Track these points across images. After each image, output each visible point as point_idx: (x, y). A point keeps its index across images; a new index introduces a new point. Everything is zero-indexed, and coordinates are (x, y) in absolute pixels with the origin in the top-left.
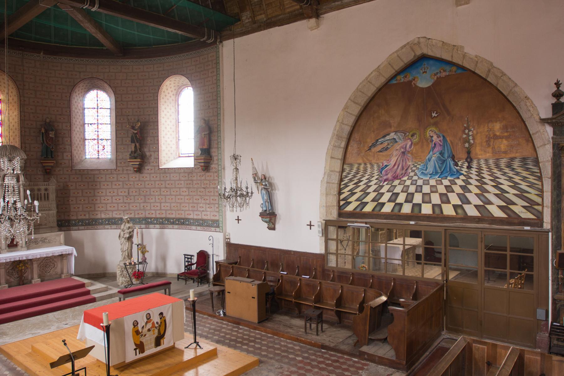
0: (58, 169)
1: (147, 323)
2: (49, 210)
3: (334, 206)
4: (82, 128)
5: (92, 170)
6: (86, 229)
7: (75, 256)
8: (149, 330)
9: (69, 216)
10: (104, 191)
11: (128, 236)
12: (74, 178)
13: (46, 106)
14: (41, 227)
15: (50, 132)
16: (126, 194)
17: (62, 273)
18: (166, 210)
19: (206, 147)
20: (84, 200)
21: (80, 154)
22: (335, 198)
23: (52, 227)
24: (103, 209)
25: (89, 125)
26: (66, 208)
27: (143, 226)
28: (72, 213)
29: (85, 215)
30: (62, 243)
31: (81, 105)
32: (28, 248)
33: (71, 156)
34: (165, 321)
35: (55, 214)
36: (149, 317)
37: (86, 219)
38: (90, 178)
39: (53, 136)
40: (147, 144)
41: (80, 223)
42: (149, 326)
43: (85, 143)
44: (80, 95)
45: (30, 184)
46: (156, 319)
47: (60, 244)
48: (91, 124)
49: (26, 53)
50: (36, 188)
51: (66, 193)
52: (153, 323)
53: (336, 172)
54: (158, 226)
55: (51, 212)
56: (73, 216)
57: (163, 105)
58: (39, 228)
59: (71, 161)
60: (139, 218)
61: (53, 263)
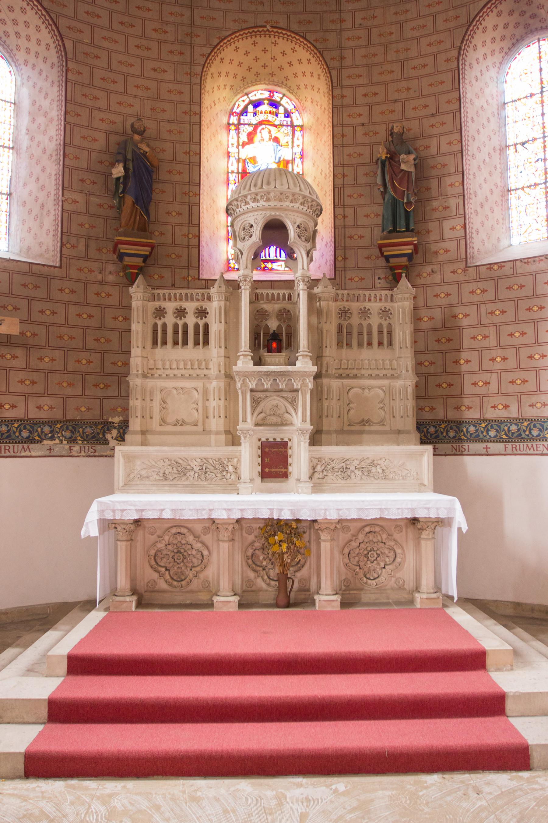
0: (428, 269)
5: (526, 261)
6: (509, 451)
7: (460, 529)
9: (458, 408)
12: (473, 292)
13: (396, 101)
14: (367, 428)
15: (403, 156)
17: (417, 589)
20: (504, 359)
21: (493, 228)
23: (399, 432)
25: (519, 147)
26: (450, 385)
28: (467, 401)
29: (506, 407)
30: (426, 483)
32: (317, 488)
35: (410, 390)
37: (511, 421)
38: (521, 287)
39: (412, 169)
41: (492, 433)
47: (420, 488)
48: (523, 144)
50: (355, 306)
51: (449, 340)
55: (399, 383)
56: (469, 408)
58: (361, 432)
59: (463, 242)
61: (392, 549)
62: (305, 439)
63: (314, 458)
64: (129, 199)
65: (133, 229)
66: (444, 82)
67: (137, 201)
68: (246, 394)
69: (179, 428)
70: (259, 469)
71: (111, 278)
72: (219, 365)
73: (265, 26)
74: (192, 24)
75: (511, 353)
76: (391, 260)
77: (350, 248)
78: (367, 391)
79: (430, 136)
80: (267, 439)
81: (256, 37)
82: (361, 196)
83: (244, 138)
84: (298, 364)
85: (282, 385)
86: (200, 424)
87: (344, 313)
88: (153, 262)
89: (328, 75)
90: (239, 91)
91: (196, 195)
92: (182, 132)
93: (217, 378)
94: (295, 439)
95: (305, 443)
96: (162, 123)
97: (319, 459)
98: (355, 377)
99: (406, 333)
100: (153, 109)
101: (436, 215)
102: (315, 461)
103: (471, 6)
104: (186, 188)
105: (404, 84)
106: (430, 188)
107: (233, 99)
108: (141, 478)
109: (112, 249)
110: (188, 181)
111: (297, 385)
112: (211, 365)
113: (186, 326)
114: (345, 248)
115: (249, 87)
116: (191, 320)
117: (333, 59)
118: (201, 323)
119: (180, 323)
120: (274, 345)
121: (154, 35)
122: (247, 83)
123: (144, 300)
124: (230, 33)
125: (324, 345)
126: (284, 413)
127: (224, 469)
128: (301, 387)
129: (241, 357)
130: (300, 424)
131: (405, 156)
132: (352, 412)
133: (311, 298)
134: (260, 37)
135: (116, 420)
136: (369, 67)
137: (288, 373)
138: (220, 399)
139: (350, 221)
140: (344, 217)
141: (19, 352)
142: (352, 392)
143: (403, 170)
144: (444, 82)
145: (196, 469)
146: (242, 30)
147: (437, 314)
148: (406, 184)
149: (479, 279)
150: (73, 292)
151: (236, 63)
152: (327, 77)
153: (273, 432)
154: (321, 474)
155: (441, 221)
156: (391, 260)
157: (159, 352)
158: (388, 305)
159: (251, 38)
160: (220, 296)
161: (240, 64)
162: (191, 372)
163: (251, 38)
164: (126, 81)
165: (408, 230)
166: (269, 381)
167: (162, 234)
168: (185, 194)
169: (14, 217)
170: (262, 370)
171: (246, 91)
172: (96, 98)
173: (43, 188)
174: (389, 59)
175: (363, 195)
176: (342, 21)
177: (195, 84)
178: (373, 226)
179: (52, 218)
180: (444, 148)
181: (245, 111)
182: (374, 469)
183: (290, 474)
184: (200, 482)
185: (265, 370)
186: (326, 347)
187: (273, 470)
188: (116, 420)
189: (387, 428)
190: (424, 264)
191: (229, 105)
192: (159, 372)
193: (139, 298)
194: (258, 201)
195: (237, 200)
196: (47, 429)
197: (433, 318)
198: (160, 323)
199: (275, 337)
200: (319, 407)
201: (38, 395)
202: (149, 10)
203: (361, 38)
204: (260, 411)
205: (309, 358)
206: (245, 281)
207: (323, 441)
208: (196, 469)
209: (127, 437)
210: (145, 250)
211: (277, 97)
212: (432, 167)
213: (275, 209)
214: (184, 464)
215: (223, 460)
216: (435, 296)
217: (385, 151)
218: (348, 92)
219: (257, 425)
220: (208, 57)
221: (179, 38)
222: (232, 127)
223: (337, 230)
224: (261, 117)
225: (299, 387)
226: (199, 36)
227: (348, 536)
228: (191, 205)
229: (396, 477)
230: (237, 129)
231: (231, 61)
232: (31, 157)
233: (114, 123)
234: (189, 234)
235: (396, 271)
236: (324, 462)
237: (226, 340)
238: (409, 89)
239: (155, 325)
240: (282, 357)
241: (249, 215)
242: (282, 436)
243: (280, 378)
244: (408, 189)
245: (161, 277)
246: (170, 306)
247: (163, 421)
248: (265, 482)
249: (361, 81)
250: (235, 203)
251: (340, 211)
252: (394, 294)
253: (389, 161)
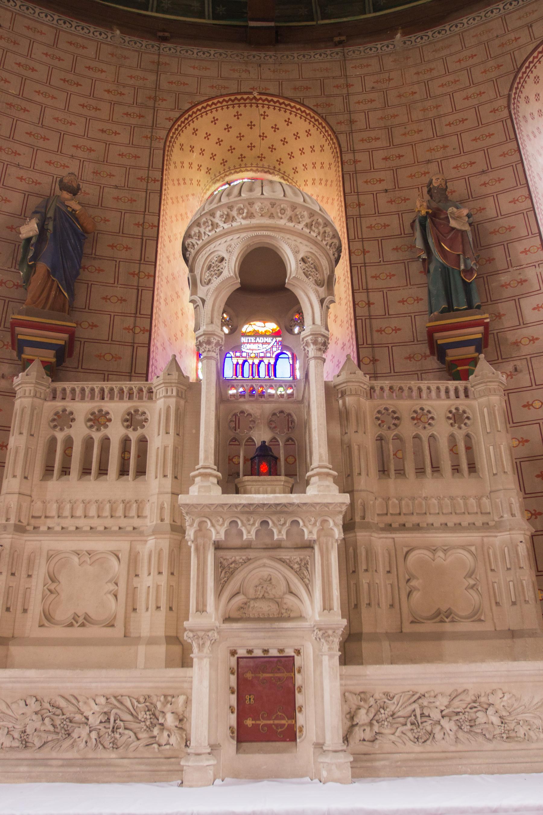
2: (486, 526)
13: (429, 162)
14: (448, 627)
23: (513, 634)
35: (523, 550)
39: (467, 228)
45: (372, 388)
49: (351, 48)
58: (439, 637)
62: (330, 649)
63: (350, 692)
64: (42, 267)
65: (44, 308)
66: (493, 134)
67: (53, 271)
68: (204, 553)
69: (76, 632)
70: (233, 719)
72: (162, 508)
73: (251, 93)
74: (157, 87)
76: (450, 352)
77: (381, 345)
78: (440, 554)
79: (486, 196)
80: (250, 652)
81: (239, 107)
82: (391, 276)
85: (280, 532)
86: (120, 623)
88: (75, 365)
89: (335, 141)
90: (218, 178)
91: (149, 276)
92: (135, 201)
93: (156, 532)
94: (309, 650)
95: (331, 657)
96: (106, 190)
97: (363, 696)
98: (417, 527)
99: (500, 448)
100: (95, 173)
101: (508, 292)
102: (354, 701)
103: (516, 53)
104: (135, 268)
105: (438, 143)
106: (493, 259)
107: (210, 187)
109: (10, 343)
110: (139, 259)
111: (311, 532)
112: (147, 512)
113: (106, 442)
114: (373, 346)
115: (231, 173)
117: (340, 123)
118: (134, 436)
119: (97, 436)
121: (106, 96)
122: (229, 168)
123: (35, 396)
124: (207, 98)
125: (356, 471)
126: (285, 594)
128: (319, 537)
129: (198, 479)
130: (320, 615)
131: (455, 210)
132: (416, 595)
134: (245, 106)
136: (389, 130)
137: (291, 509)
138: (160, 573)
139: (378, 309)
140: (369, 304)
142: (412, 557)
143: (453, 229)
144: (493, 134)
145: (94, 721)
146: (222, 96)
148: (461, 246)
151: (213, 139)
152: (334, 143)
153: (262, 634)
154: (368, 729)
155: (517, 300)
156: (450, 352)
158: (462, 403)
159: (233, 107)
160: (169, 389)
161: (219, 142)
162: (109, 522)
163: (233, 107)
164: (61, 140)
165: (470, 306)
166: (254, 524)
167: (93, 326)
168: (133, 274)
170: (238, 502)
171: (227, 179)
172: (16, 153)
174: (414, 118)
175: (394, 275)
176: (348, 86)
177: (157, 149)
178: (413, 315)
180: (506, 207)
182: (481, 717)
183: (301, 731)
184: (102, 754)
185: (244, 502)
186: (360, 474)
187: (262, 722)
189: (487, 627)
190: (500, 360)
191: (205, 193)
192: (50, 523)
193: (27, 394)
194: (234, 219)
195: (199, 225)
197: (527, 441)
198: (60, 436)
200: (353, 587)
202: (102, 71)
203: (374, 100)
204: (236, 589)
205: (331, 479)
206: (209, 343)
207: (364, 655)
208: (94, 721)
212: (491, 233)
214: (69, 709)
215: (154, 700)
216: (524, 406)
217: (425, 204)
219: (228, 619)
221: (139, 101)
223: (359, 322)
225: (315, 537)
226: (165, 100)
228: (140, 289)
229: (531, 733)
231: (208, 136)
234: (135, 327)
235: (459, 368)
236: (372, 701)
237: (175, 465)
238: (445, 147)
239: (53, 441)
241: (219, 242)
242: (281, 643)
243: (274, 518)
244: (464, 253)
248: (245, 752)
249: (378, 144)
250: (196, 230)
251: (361, 297)
252: (469, 386)
253: (432, 220)
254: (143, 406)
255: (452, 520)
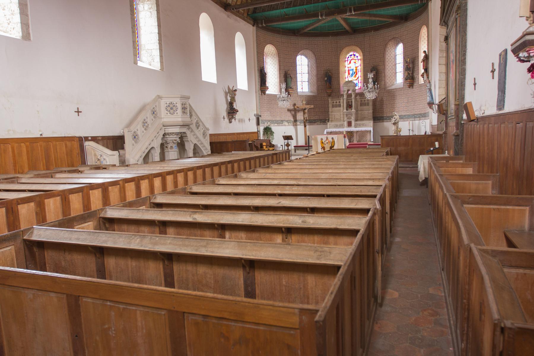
1: (326, 140)
3: (443, 95)
4: (394, 66)
5: (393, 89)
8: (327, 143)
9: (383, 114)
10: (398, 100)
11: (393, 122)
16: (407, 101)
18: (421, 109)
19: (424, 68)
22: (444, 89)
23: (370, 119)
24: (397, 110)
26: (382, 110)
27: (413, 119)
28: (384, 113)
31: (394, 54)
32: (355, 128)
33: (385, 83)
34: (334, 141)
36: (327, 138)
40: (415, 71)
41: (388, 118)
42: (327, 141)
43: (396, 75)
44: (392, 48)
46: (330, 140)
47: (371, 127)
52: (329, 141)
53: (443, 73)
54: (418, 119)
55: (370, 111)
57: (423, 45)
58: (364, 119)
60: (412, 115)
64: (328, 83)
71: (326, 96)
75: (391, 105)
79: (380, 66)
83: (349, 63)
84: (352, 110)
87: (361, 101)
98: (363, 111)
101: (381, 80)
108: (331, 127)
113: (337, 104)
116: (338, 103)
117: (363, 50)
120: (350, 107)
127: (343, 125)
133: (356, 99)
135: (327, 119)
141: (312, 109)
147: (380, 98)
149: (386, 92)
150: (320, 99)
155: (381, 81)
157: (333, 108)
169: (309, 85)
173: (314, 81)
179: (316, 87)
181: (348, 57)
188: (327, 119)
196: (317, 121)
199: (350, 106)
201: (316, 116)
209: (329, 121)
210: (331, 91)
211: (355, 53)
213: (348, 88)
218: (366, 57)
220: (340, 53)
222: (346, 61)
224: (352, 58)
227: (359, 134)
230: (347, 61)
232: (311, 75)
233: (325, 69)
239: (333, 105)
240: (351, 109)
245: (334, 94)
246: (335, 101)
247: (334, 119)
254: (340, 101)
255: (366, 110)
